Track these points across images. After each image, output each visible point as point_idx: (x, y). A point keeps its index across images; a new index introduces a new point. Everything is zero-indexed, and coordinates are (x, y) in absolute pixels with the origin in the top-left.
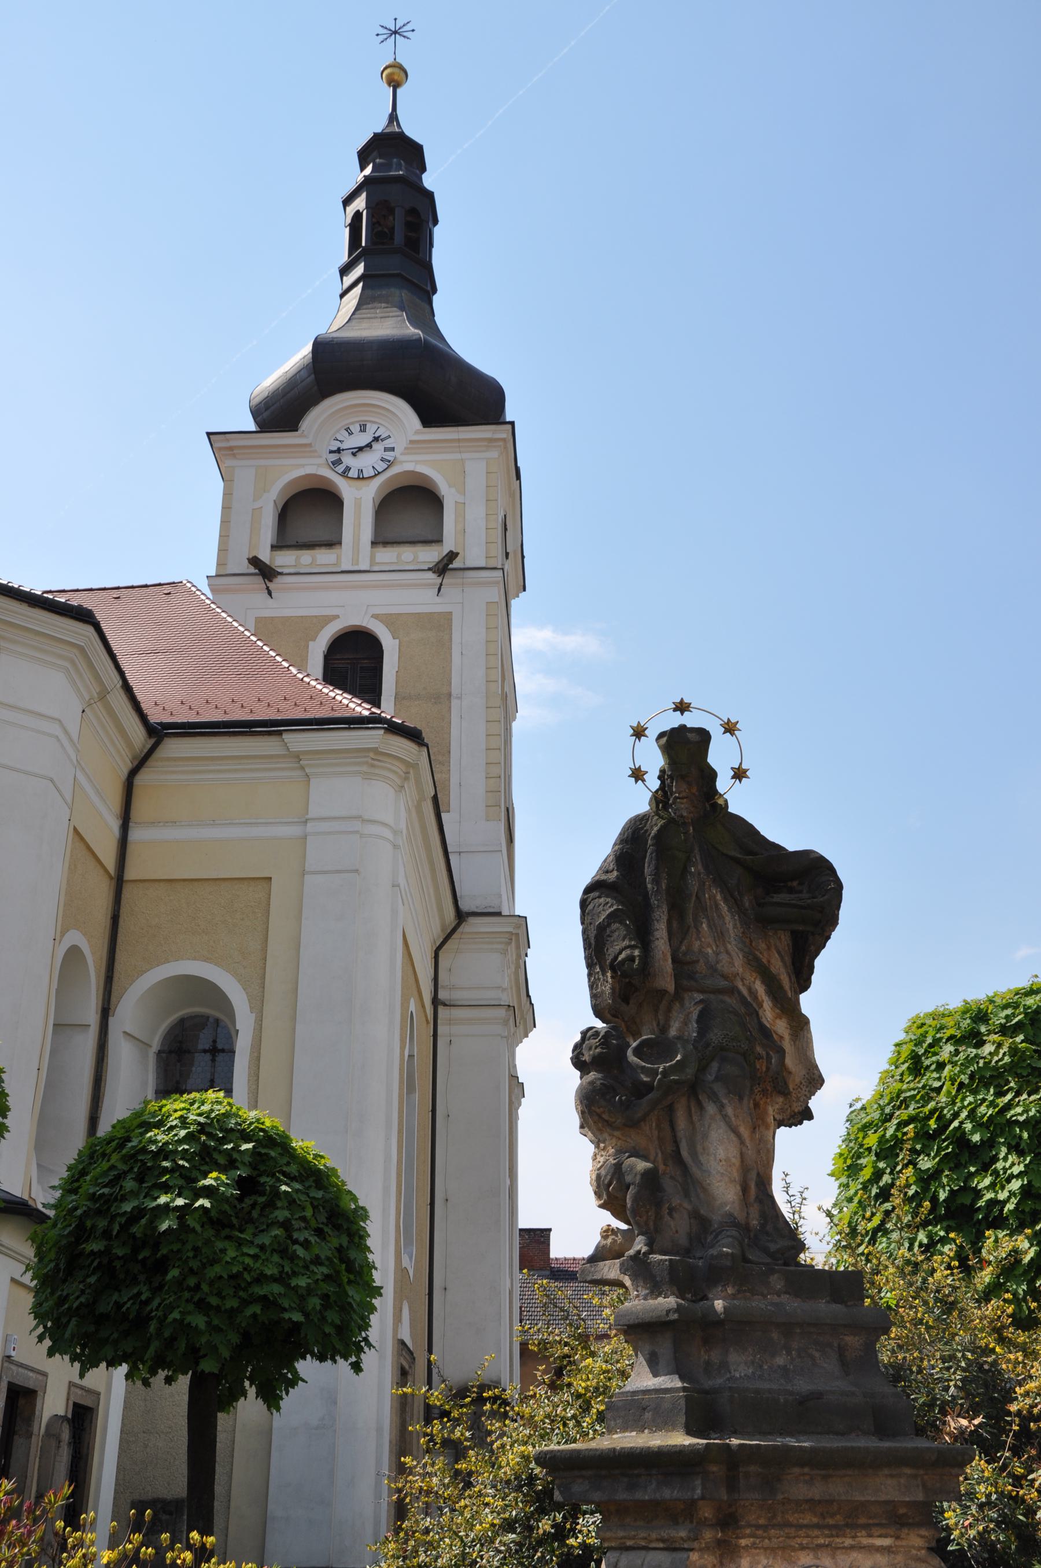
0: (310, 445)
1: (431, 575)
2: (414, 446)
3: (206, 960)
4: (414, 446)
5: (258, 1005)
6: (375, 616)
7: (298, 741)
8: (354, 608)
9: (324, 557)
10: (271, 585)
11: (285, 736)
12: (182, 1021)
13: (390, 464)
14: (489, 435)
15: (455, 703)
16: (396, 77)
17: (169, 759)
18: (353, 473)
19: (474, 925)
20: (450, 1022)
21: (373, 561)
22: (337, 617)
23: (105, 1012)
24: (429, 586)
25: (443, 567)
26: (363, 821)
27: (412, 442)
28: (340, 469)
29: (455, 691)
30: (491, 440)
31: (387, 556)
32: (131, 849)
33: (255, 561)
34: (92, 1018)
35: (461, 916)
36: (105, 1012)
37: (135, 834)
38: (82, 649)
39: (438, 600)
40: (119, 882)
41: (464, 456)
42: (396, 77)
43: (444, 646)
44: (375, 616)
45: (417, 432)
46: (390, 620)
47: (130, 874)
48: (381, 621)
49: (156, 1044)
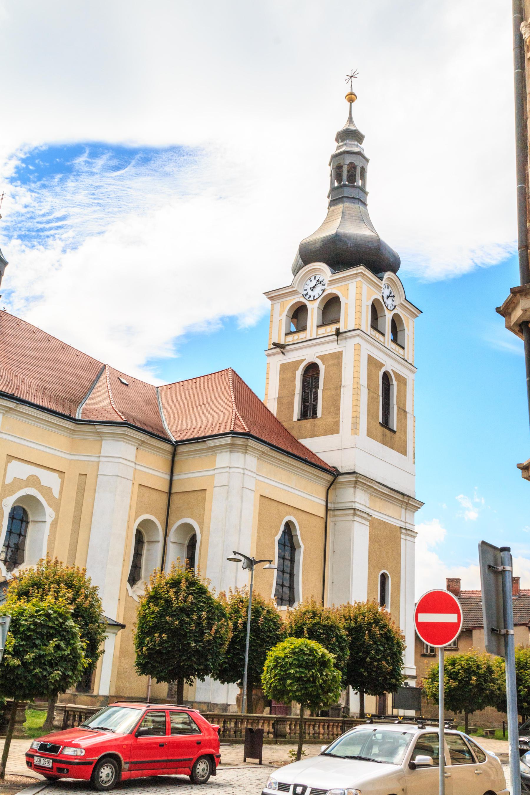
0: (296, 290)
1: (335, 337)
2: (331, 282)
3: (191, 517)
4: (331, 282)
6: (317, 357)
7: (211, 443)
8: (309, 355)
9: (302, 336)
10: (284, 351)
11: (207, 442)
13: (324, 291)
14: (355, 272)
15: (342, 390)
16: (351, 98)
18: (312, 298)
19: (342, 479)
20: (335, 516)
21: (317, 335)
22: (305, 359)
24: (333, 341)
25: (338, 333)
26: (230, 468)
27: (329, 281)
28: (307, 297)
29: (343, 384)
30: (356, 274)
31: (323, 331)
32: (174, 482)
33: (274, 344)
34: (161, 538)
37: (175, 478)
39: (338, 346)
40: (170, 493)
41: (347, 282)
42: (351, 98)
43: (339, 366)
44: (317, 357)
45: (330, 277)
46: (322, 358)
47: (173, 491)
48: (320, 359)
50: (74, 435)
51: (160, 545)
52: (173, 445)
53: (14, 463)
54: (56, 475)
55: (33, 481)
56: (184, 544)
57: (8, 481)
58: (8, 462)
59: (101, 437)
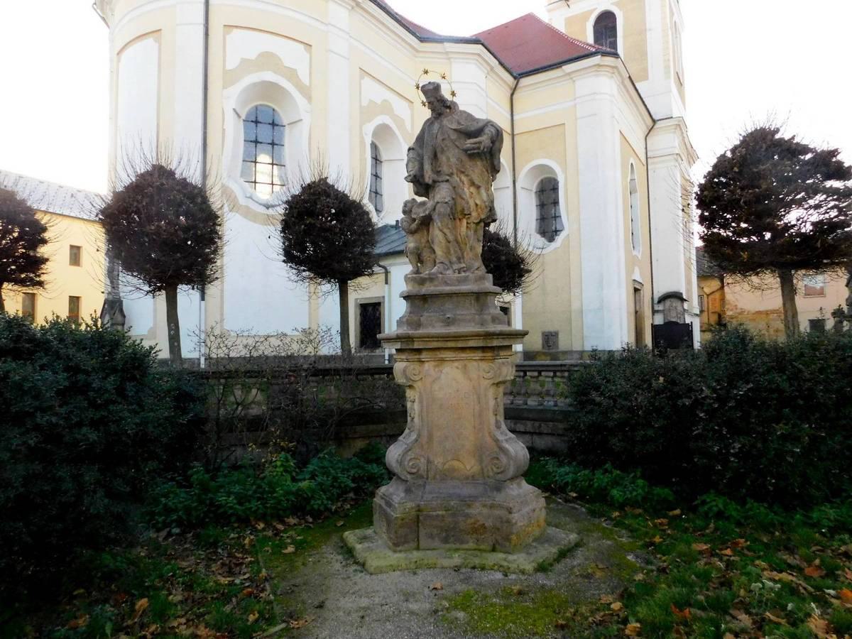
3: (546, 158)
5: (565, 171)
6: (613, 4)
12: (542, 181)
17: (524, 86)
20: (653, 163)
23: (514, 182)
29: (648, 26)
35: (654, 121)
36: (514, 182)
37: (515, 118)
38: (479, 55)
44: (613, 4)
49: (534, 190)
50: (416, 57)
51: (510, 191)
52: (515, 78)
53: (367, 80)
54: (405, 104)
55: (386, 108)
56: (531, 190)
57: (365, 103)
58: (362, 78)
59: (449, 59)
